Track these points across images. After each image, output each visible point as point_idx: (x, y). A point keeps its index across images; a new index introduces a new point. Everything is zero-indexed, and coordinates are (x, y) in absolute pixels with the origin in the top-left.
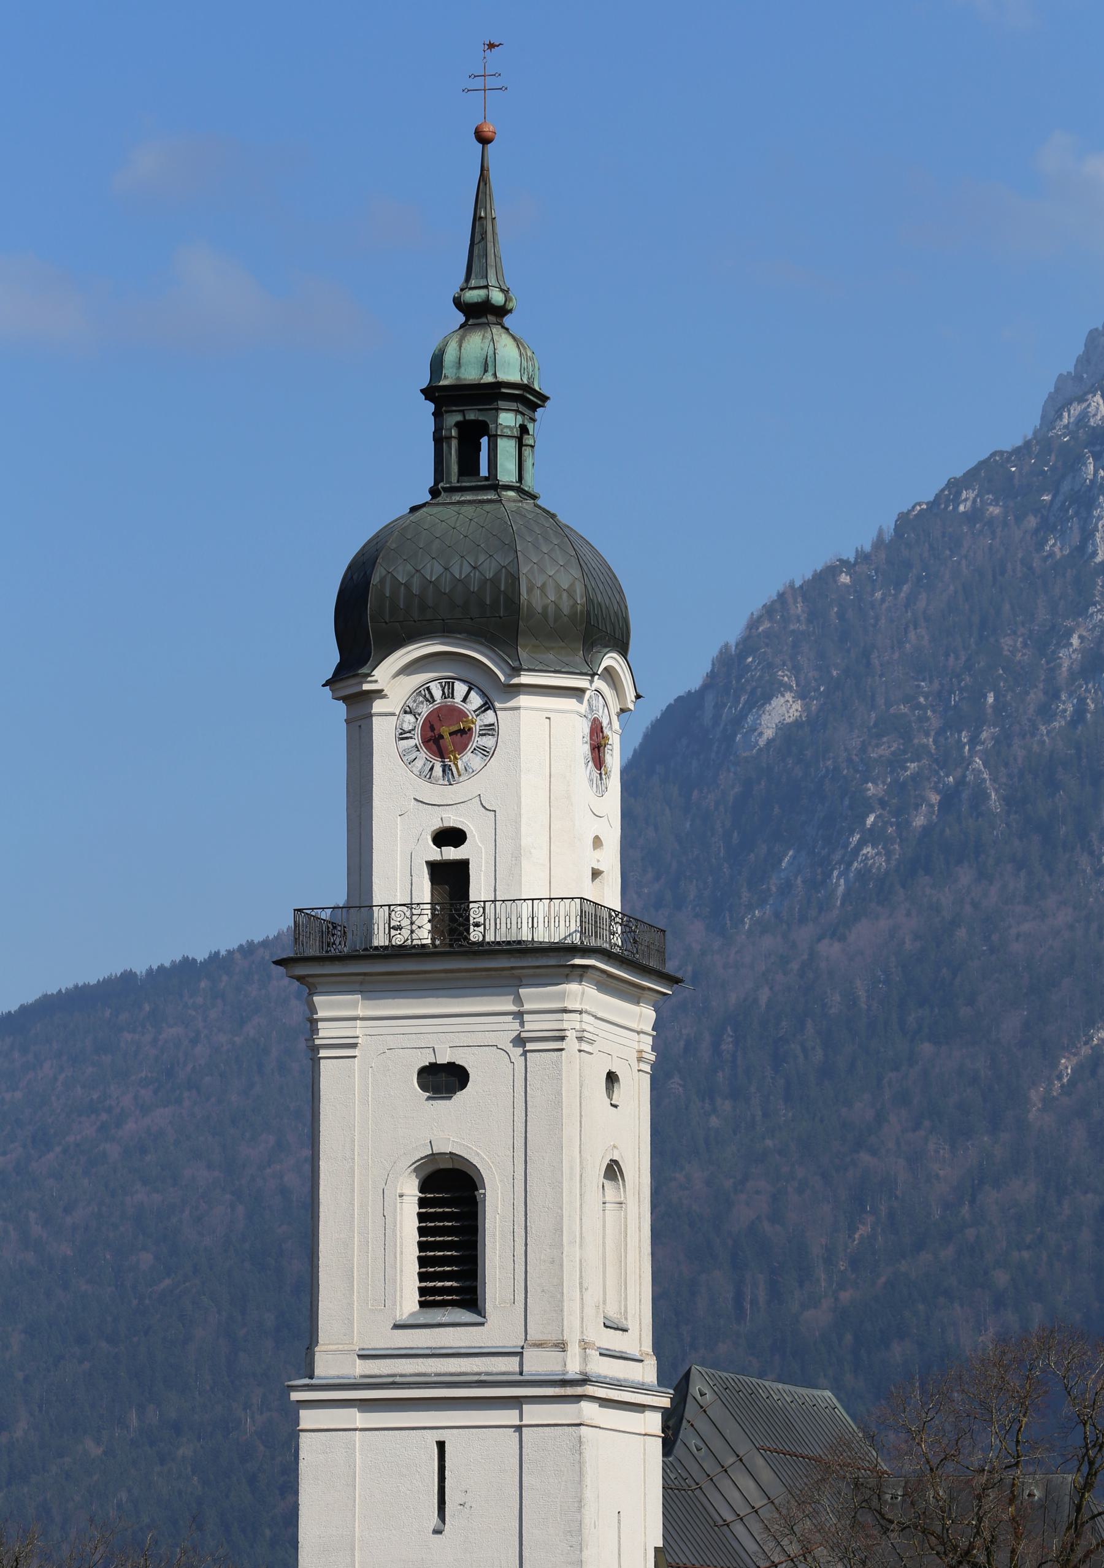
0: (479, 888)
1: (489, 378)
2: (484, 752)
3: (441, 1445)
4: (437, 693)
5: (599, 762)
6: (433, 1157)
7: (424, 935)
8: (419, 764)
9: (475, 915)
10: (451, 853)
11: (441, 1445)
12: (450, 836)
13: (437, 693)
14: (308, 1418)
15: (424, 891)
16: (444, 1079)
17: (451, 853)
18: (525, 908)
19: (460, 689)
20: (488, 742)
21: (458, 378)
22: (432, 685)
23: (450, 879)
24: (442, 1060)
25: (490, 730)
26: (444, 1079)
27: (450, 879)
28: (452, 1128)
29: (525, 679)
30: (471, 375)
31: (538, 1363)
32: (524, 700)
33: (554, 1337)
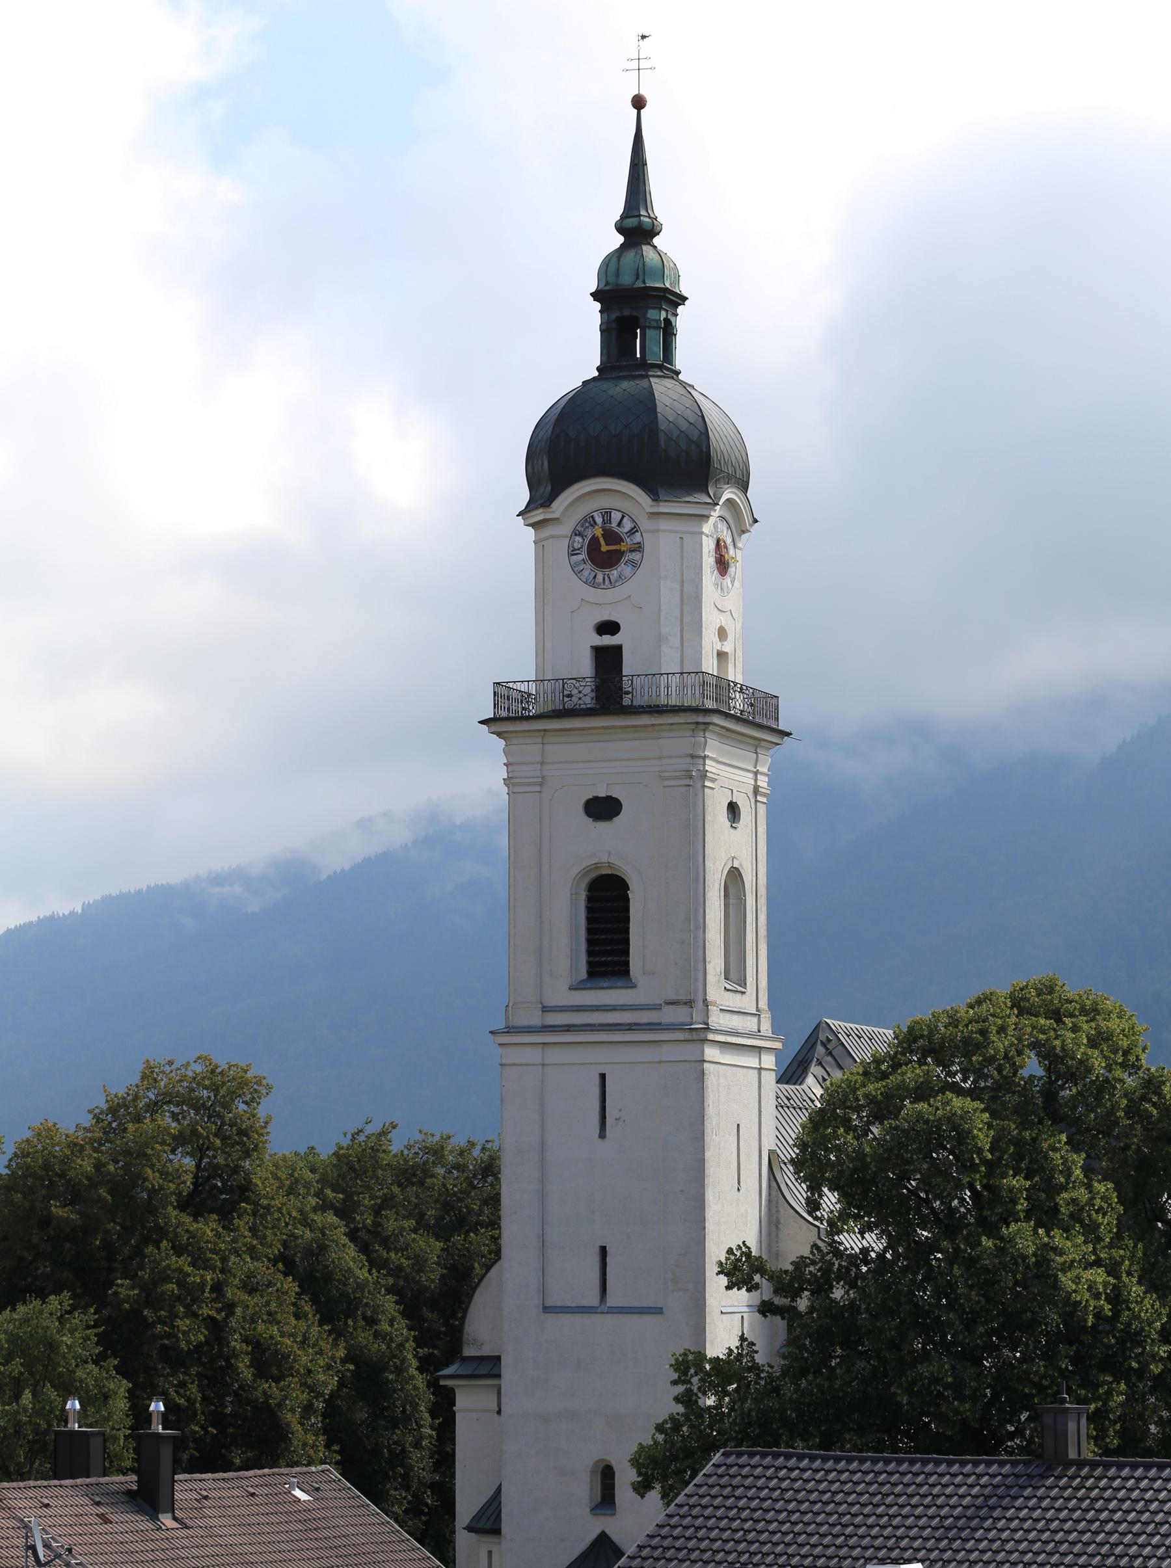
1: (640, 284)
3: (603, 1076)
4: (599, 520)
6: (596, 866)
7: (588, 700)
8: (586, 573)
9: (626, 684)
10: (607, 640)
11: (603, 1076)
12: (608, 627)
13: (599, 520)
16: (603, 808)
17: (607, 640)
18: (663, 679)
19: (616, 516)
20: (636, 556)
21: (617, 285)
22: (595, 514)
23: (608, 661)
24: (602, 794)
25: (638, 548)
26: (603, 808)
27: (608, 661)
28: (606, 845)
29: (664, 508)
30: (627, 280)
31: (670, 1015)
32: (663, 524)
33: (683, 997)
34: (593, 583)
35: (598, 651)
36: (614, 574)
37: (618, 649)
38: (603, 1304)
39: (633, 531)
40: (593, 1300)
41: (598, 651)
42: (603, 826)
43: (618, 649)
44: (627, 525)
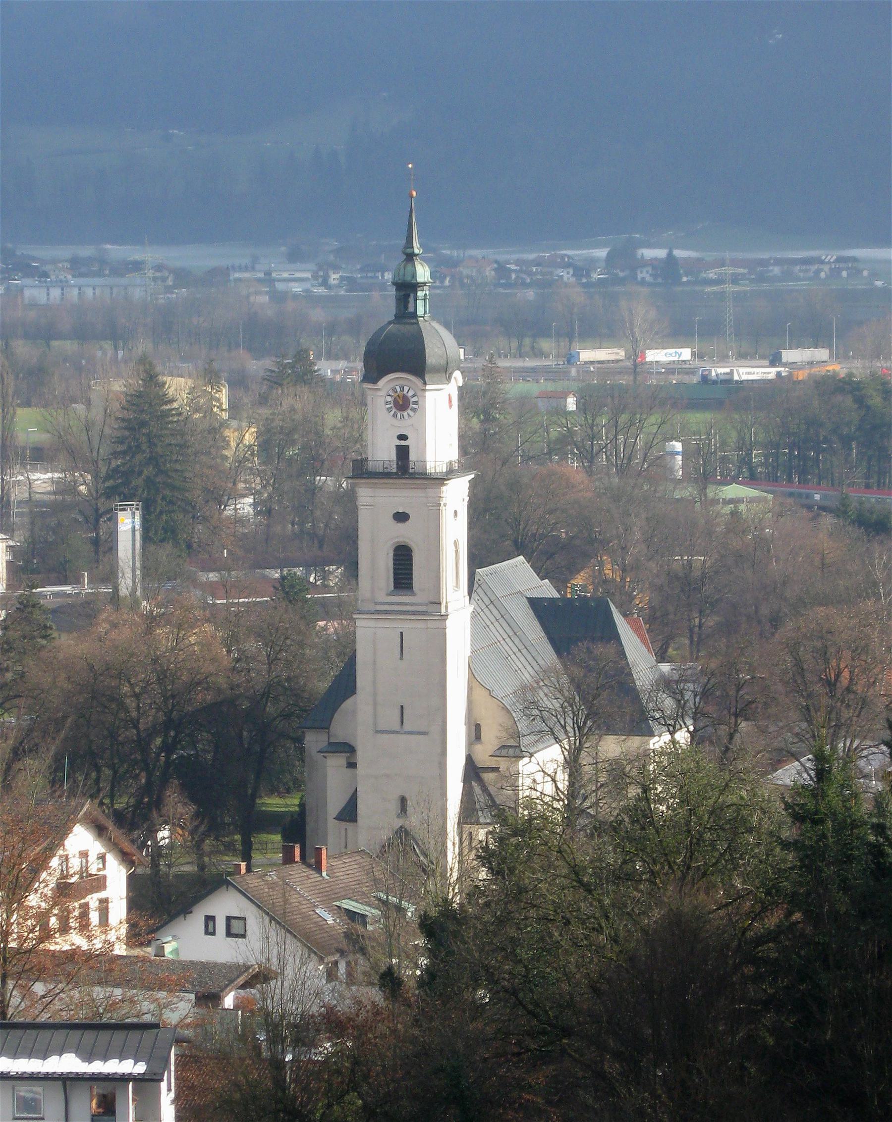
0: (413, 456)
2: (414, 410)
3: (402, 633)
4: (398, 390)
5: (451, 406)
10: (403, 443)
11: (402, 633)
12: (402, 437)
13: (398, 390)
14: (358, 623)
15: (394, 457)
16: (401, 517)
17: (403, 443)
19: (406, 389)
23: (403, 452)
26: (401, 517)
27: (403, 452)
34: (395, 416)
35: (399, 448)
36: (405, 414)
37: (408, 447)
38: (401, 728)
39: (413, 396)
40: (397, 727)
41: (399, 448)
42: (400, 525)
43: (408, 447)
44: (411, 393)
